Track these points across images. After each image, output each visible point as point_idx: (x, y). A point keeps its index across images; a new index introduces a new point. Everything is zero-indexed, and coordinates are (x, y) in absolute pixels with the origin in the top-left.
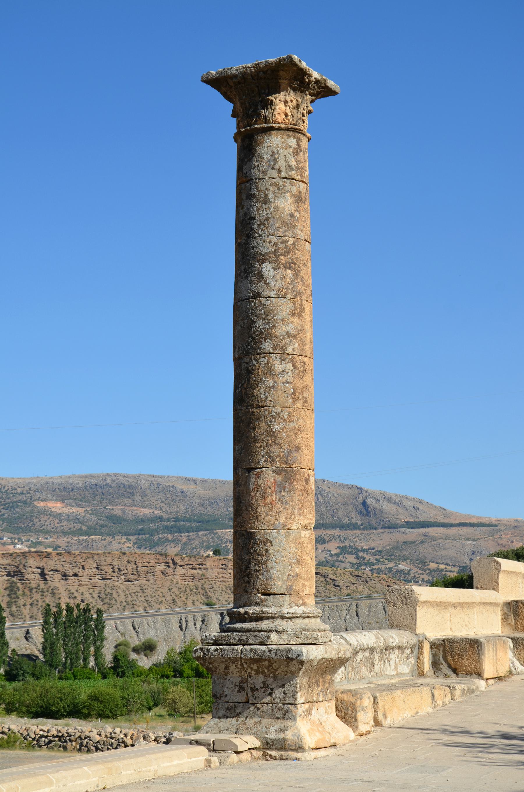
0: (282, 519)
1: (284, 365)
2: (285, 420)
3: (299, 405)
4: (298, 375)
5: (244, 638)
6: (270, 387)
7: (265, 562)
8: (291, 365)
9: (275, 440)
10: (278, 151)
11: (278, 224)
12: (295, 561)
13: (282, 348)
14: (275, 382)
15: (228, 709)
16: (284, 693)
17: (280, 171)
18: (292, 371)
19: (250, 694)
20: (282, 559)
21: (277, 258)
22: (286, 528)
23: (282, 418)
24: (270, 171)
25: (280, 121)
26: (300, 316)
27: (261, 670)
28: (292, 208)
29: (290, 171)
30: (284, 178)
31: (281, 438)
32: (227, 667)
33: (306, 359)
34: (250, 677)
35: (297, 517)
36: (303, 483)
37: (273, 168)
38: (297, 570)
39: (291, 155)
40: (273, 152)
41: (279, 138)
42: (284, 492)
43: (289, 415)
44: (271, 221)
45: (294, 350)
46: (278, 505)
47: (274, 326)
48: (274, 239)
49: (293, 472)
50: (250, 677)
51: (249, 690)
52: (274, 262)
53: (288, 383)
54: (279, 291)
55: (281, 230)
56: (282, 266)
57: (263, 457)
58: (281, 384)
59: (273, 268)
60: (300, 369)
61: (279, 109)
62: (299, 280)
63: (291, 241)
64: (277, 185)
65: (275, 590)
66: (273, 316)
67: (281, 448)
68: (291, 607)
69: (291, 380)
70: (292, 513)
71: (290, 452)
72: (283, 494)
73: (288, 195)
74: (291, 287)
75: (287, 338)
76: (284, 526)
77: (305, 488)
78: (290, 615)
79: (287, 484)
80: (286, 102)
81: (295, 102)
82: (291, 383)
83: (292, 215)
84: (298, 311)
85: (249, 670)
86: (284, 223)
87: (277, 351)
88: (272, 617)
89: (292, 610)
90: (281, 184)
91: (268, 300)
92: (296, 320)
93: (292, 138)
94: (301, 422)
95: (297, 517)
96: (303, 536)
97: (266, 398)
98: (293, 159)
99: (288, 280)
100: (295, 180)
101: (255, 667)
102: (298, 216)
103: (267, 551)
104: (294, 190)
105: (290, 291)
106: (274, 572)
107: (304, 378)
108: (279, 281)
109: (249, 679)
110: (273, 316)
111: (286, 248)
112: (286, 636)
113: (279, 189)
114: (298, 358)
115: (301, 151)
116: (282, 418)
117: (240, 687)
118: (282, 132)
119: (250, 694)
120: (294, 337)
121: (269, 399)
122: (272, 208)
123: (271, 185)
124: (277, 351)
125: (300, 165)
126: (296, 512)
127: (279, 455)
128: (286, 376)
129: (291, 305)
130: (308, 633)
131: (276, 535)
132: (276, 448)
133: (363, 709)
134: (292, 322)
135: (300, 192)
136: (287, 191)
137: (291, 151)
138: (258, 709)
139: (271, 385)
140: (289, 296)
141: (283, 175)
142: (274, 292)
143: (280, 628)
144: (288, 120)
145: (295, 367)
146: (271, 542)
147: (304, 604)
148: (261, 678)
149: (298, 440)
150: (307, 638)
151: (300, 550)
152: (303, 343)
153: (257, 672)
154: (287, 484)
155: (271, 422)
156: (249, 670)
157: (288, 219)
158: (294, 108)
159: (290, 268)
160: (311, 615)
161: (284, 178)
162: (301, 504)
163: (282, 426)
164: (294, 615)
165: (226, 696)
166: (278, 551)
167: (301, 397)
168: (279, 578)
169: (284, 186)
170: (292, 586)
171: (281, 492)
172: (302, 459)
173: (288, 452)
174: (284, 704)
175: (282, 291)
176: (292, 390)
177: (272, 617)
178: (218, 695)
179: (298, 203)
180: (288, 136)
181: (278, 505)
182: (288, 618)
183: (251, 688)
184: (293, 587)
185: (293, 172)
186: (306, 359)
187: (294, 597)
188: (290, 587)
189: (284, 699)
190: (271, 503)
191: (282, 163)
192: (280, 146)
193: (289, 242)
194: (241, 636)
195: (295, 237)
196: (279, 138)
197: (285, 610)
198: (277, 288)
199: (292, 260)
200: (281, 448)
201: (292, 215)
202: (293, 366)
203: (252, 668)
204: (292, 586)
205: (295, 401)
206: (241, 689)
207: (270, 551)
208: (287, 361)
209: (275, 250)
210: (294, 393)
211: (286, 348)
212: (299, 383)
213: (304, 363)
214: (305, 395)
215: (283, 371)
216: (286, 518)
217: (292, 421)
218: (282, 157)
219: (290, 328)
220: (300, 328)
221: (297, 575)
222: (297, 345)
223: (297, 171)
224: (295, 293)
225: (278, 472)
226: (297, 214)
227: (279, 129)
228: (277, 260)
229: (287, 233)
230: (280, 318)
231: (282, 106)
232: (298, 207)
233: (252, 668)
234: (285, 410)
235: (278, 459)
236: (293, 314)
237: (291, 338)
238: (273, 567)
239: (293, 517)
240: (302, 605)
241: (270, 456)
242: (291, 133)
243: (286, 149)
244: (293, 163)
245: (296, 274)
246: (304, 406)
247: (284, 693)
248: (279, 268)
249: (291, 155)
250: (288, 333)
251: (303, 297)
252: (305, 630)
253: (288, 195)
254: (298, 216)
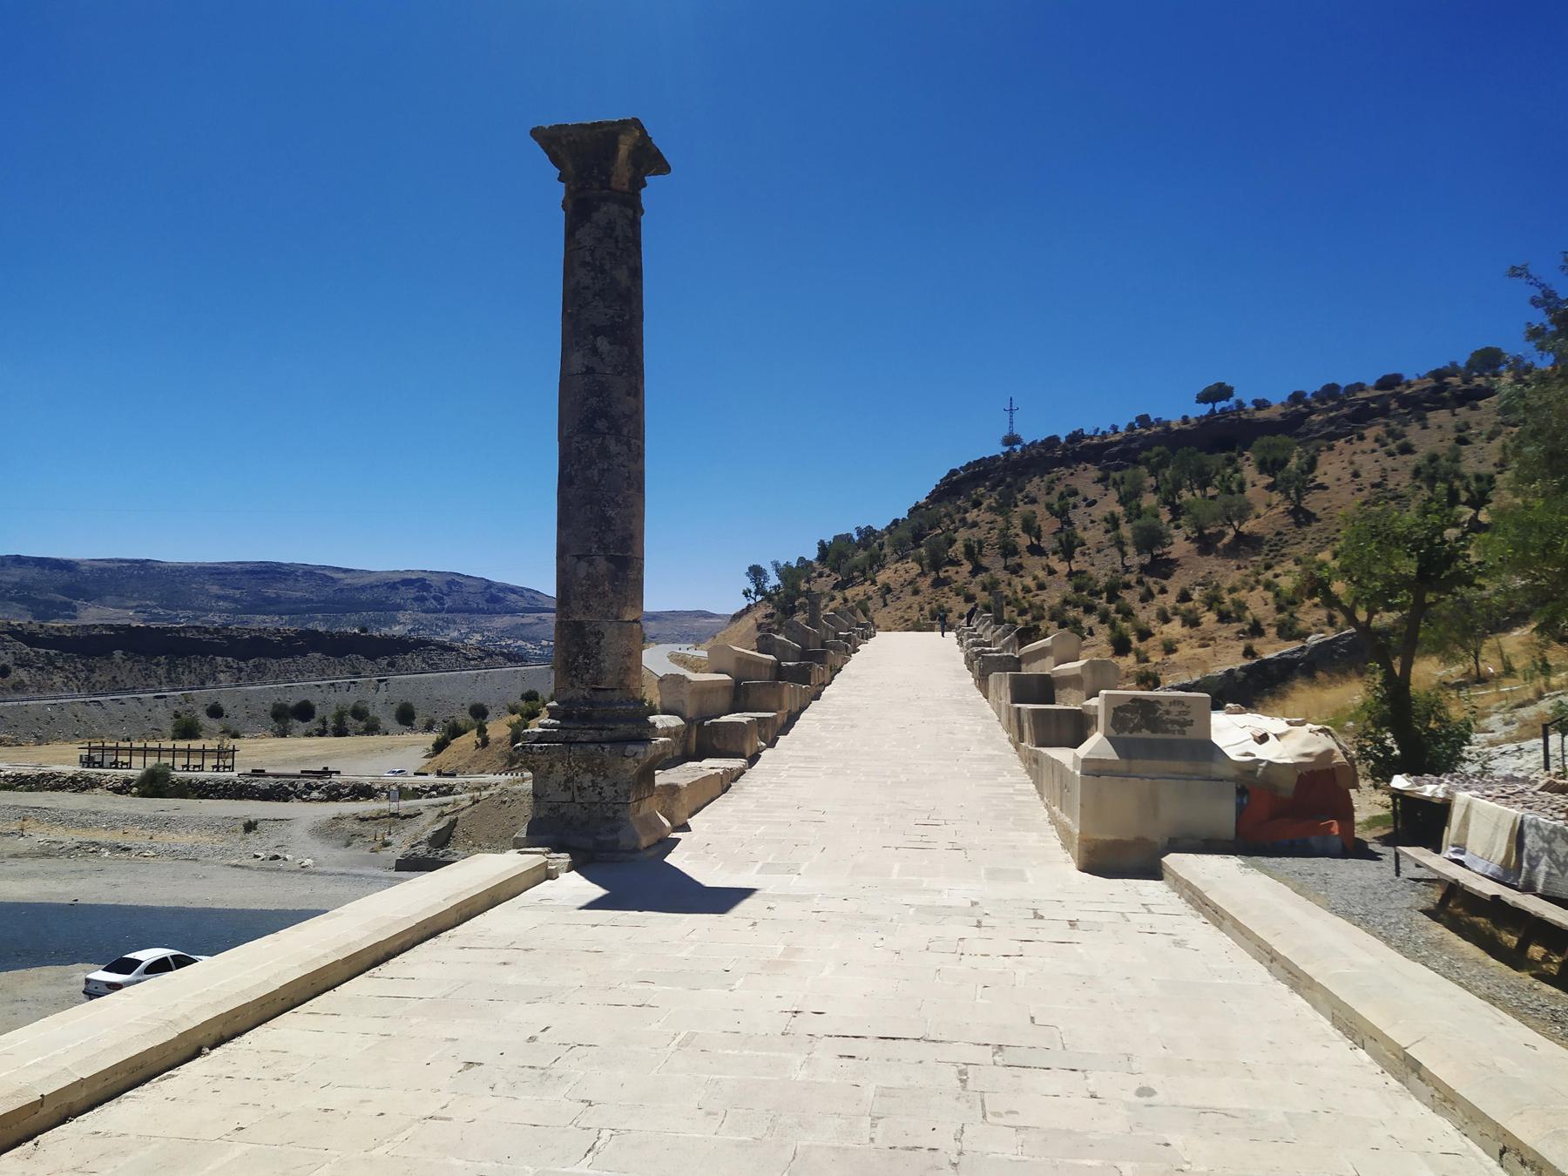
5: (572, 735)
6: (604, 470)
15: (551, 809)
16: (616, 791)
17: (617, 241)
19: (576, 793)
23: (616, 503)
27: (590, 769)
31: (615, 525)
32: (551, 766)
34: (577, 776)
45: (629, 432)
50: (577, 776)
51: (576, 789)
53: (623, 466)
57: (596, 542)
58: (616, 467)
79: (620, 574)
85: (577, 769)
101: (584, 766)
103: (598, 643)
109: (576, 778)
114: (633, 441)
116: (616, 503)
117: (566, 786)
119: (576, 793)
121: (603, 482)
138: (586, 809)
146: (603, 634)
148: (589, 777)
153: (586, 771)
156: (577, 769)
165: (549, 795)
174: (614, 804)
176: (627, 475)
178: (540, 795)
183: (578, 787)
184: (625, 681)
188: (621, 682)
189: (615, 797)
194: (569, 733)
200: (615, 535)
203: (580, 767)
204: (622, 680)
206: (567, 788)
215: (619, 453)
233: (580, 767)
247: (616, 791)
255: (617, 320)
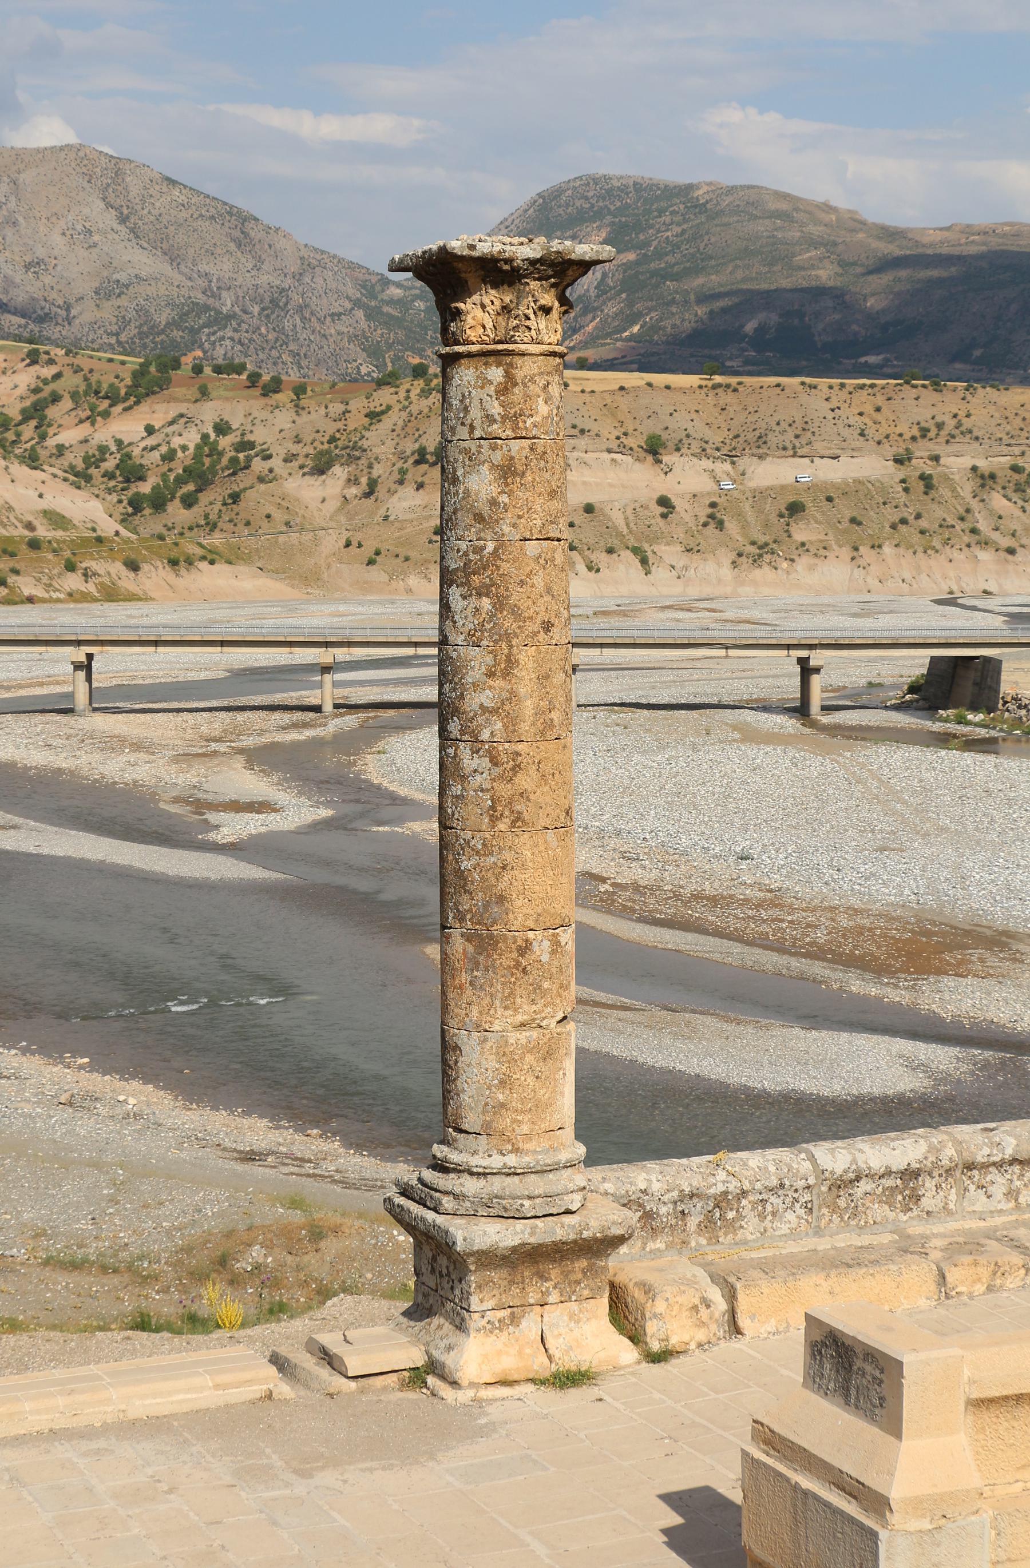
0: (475, 1014)
1: (476, 761)
2: (478, 853)
3: (502, 826)
4: (501, 777)
6: (457, 797)
7: (455, 1080)
8: (488, 759)
9: (465, 885)
10: (470, 392)
11: (469, 519)
12: (496, 1082)
13: (473, 731)
14: (463, 789)
17: (472, 428)
18: (490, 770)
20: (475, 1079)
21: (467, 580)
22: (480, 1029)
23: (473, 850)
24: (459, 428)
25: (474, 339)
26: (506, 674)
28: (494, 490)
29: (488, 426)
30: (479, 439)
33: (520, 747)
35: (500, 1011)
36: (515, 955)
37: (463, 424)
38: (501, 1097)
39: (491, 396)
40: (463, 396)
41: (472, 370)
42: (477, 971)
43: (484, 845)
44: (459, 514)
46: (469, 991)
47: (462, 694)
48: (463, 545)
49: (491, 937)
52: (462, 585)
53: (482, 790)
54: (469, 635)
55: (473, 530)
56: (474, 592)
58: (472, 793)
59: (461, 595)
60: (505, 766)
61: (474, 318)
62: (505, 613)
63: (490, 546)
64: (467, 451)
65: (465, 1126)
66: (461, 678)
67: (473, 899)
68: (490, 1156)
69: (487, 785)
70: (492, 1005)
71: (487, 906)
72: (476, 973)
73: (485, 469)
74: (488, 626)
75: (481, 715)
76: (478, 1026)
77: (518, 964)
78: (481, 1170)
79: (481, 958)
80: (483, 306)
81: (497, 303)
82: (488, 790)
83: (493, 503)
84: (503, 666)
86: (479, 518)
87: (466, 737)
88: (458, 1170)
89: (485, 1162)
90: (474, 450)
91: (455, 650)
92: (498, 683)
93: (493, 368)
94: (508, 856)
95: (500, 1011)
96: (512, 1041)
97: (453, 814)
98: (496, 404)
99: (484, 615)
100: (500, 439)
102: (507, 500)
103: (456, 1062)
104: (498, 457)
105: (486, 634)
106: (465, 1098)
107: (516, 780)
108: (470, 618)
110: (461, 678)
111: (481, 560)
112: (468, 1204)
113: (470, 459)
115: (516, 384)
116: (473, 850)
118: (475, 359)
120: (494, 711)
121: (456, 816)
122: (461, 491)
123: (460, 452)
124: (466, 737)
125: (512, 411)
126: (497, 1003)
127: (470, 911)
128: (478, 778)
129: (489, 659)
130: (504, 1202)
131: (466, 1040)
132: (466, 897)
133: (655, 1316)
134: (490, 687)
135: (512, 458)
136: (484, 462)
137: (491, 389)
139: (459, 793)
140: (484, 643)
141: (477, 434)
142: (462, 637)
143: (457, 1190)
144: (488, 336)
145: (495, 762)
146: (461, 1051)
147: (516, 1150)
149: (502, 886)
150: (506, 1209)
151: (506, 1065)
152: (512, 722)
154: (481, 958)
155: (459, 854)
157: (486, 510)
158: (498, 314)
159: (487, 595)
160: (519, 1171)
161: (479, 439)
162: (507, 992)
163: (473, 862)
164: (487, 1171)
166: (469, 1066)
167: (507, 813)
168: (472, 1109)
169: (479, 452)
170: (492, 1121)
171: (472, 970)
172: (511, 916)
173: (484, 905)
175: (474, 635)
176: (490, 803)
177: (458, 1170)
179: (506, 479)
180: (486, 364)
181: (469, 991)
182: (479, 1174)
184: (495, 1124)
185: (495, 426)
186: (520, 747)
187: (494, 1141)
188: (487, 1125)
190: (460, 988)
191: (475, 414)
192: (473, 383)
193: (487, 550)
195: (501, 543)
196: (472, 370)
197: (477, 1162)
198: (467, 629)
199: (491, 579)
200: (473, 899)
201: (493, 503)
202: (491, 761)
204: (492, 1121)
205: (494, 820)
207: (459, 1064)
208: (481, 753)
209: (465, 564)
210: (493, 808)
211: (479, 732)
212: (504, 790)
213: (518, 754)
214: (518, 808)
215: (475, 771)
216: (481, 1013)
217: (491, 854)
218: (476, 403)
219: (486, 698)
220: (505, 695)
221: (503, 1105)
222: (499, 725)
223: (503, 423)
224: (496, 637)
225: (468, 938)
226: (504, 499)
227: (470, 355)
228: (467, 583)
229: (482, 535)
230: (470, 680)
231: (478, 312)
232: (507, 485)
234: (478, 835)
235: (468, 917)
236: (491, 674)
237: (487, 714)
238: (464, 1090)
239: (492, 1012)
240: (511, 1152)
241: (458, 910)
242: (491, 359)
243: (482, 388)
244: (496, 409)
245: (500, 604)
246: (514, 827)
248: (471, 595)
249: (491, 396)
250: (482, 706)
251: (514, 642)
252: (496, 1197)
253: (485, 469)
254: (507, 500)
255: (472, 557)
